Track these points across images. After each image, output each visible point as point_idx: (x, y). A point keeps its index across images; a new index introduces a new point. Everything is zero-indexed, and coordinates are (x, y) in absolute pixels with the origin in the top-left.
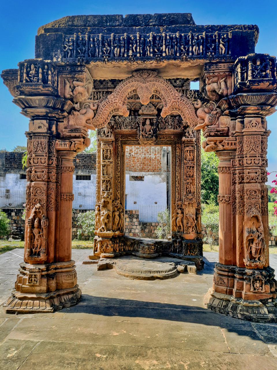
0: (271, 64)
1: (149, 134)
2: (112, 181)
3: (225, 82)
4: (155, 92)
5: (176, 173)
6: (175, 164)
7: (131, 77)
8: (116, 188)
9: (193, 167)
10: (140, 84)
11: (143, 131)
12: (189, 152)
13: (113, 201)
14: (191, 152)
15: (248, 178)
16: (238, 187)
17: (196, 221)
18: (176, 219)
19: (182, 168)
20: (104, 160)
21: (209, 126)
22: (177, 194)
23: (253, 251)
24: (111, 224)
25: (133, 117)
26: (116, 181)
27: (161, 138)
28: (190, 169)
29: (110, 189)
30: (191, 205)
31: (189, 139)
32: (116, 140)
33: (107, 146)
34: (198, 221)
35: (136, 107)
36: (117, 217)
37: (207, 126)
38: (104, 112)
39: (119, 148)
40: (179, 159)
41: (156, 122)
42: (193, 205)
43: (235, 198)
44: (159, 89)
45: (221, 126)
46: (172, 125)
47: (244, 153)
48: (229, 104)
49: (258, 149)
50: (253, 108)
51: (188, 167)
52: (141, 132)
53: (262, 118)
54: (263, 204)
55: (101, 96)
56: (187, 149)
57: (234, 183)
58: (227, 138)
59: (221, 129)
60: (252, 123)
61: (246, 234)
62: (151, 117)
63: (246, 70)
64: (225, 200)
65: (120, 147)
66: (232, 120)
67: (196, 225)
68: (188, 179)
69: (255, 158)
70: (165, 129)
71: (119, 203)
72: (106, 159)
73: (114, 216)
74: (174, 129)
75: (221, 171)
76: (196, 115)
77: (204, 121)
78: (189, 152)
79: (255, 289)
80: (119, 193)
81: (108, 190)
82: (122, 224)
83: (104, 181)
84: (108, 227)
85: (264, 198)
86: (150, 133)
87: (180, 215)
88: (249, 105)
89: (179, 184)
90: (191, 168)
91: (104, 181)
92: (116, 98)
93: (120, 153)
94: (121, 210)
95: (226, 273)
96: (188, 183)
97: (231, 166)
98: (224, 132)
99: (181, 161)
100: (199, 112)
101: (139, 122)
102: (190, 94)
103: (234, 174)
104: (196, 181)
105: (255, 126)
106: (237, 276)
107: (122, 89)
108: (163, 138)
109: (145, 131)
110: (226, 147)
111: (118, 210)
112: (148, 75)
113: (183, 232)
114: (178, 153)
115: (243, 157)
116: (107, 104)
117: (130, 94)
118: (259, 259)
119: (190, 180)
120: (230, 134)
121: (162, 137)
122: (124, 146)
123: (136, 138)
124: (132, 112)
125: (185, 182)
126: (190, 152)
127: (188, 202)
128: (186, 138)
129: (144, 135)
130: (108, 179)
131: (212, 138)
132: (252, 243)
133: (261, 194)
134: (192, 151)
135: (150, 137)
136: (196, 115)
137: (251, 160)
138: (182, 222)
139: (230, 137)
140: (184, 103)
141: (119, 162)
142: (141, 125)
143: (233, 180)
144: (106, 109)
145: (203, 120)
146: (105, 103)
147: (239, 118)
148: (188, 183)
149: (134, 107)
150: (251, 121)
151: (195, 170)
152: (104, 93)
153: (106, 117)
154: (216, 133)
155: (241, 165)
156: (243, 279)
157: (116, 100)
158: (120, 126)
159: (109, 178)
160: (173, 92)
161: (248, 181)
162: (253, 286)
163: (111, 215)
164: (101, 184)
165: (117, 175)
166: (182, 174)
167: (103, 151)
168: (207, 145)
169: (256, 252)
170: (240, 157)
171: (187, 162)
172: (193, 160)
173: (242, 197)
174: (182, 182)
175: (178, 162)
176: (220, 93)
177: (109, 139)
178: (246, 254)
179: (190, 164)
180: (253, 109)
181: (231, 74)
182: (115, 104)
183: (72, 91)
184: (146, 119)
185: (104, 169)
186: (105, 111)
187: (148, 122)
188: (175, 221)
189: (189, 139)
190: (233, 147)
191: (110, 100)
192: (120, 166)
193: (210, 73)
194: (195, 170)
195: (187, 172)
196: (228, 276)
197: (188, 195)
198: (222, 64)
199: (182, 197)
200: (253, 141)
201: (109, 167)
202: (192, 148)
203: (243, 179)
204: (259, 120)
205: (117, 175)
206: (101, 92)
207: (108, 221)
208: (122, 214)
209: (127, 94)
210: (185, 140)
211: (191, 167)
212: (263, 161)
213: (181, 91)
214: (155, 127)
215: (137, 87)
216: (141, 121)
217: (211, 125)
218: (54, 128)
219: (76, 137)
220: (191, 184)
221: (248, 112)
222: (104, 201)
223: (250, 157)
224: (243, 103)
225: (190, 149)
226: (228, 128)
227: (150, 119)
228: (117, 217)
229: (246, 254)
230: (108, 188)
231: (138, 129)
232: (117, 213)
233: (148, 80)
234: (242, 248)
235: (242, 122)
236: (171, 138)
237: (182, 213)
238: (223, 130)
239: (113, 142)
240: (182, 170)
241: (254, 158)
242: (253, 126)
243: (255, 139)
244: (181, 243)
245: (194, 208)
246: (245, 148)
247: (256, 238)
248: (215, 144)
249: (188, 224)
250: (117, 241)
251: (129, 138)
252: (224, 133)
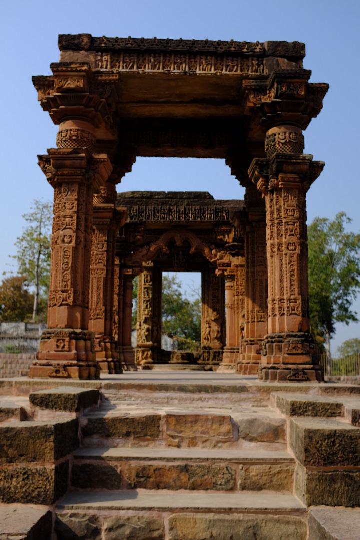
36: (155, 331)
91: (144, 301)
95: (229, 350)
183: (134, 239)
187: (181, 253)
196: (231, 352)
218: (122, 262)
219: (136, 267)
228: (155, 331)
244: (209, 352)
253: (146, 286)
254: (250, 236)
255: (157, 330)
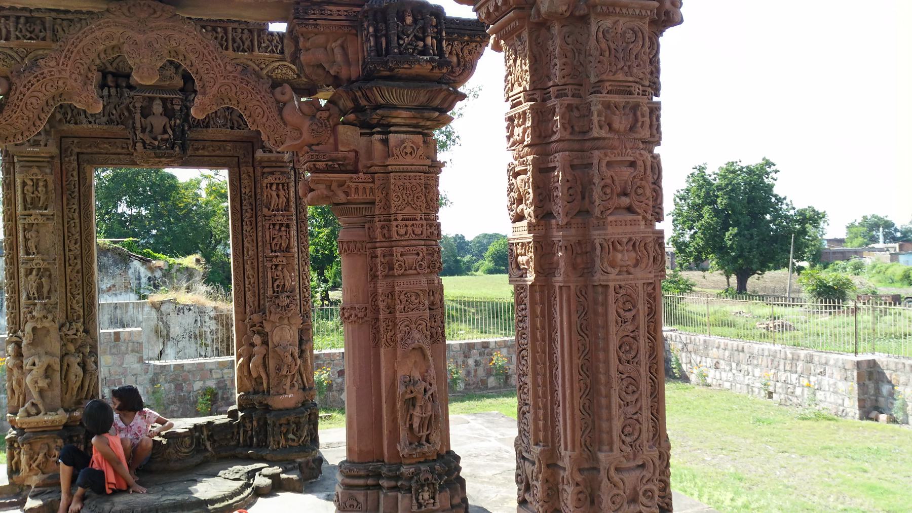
0: (434, 24)
1: (167, 140)
2: (56, 270)
3: (343, 47)
4: (173, 54)
5: (245, 241)
6: (239, 216)
7: (102, 13)
8: (69, 288)
9: (288, 226)
10: (130, 33)
11: (143, 130)
12: (274, 187)
13: (62, 326)
14: (281, 186)
15: (400, 266)
16: (382, 286)
17: (299, 361)
18: (250, 359)
19: (260, 229)
20: (27, 212)
21: (314, 148)
22: (248, 294)
23: (416, 425)
24: (57, 391)
25: (113, 91)
26: (69, 270)
27: (197, 149)
28: (280, 230)
29: (49, 292)
30: (286, 321)
31: (274, 155)
32: (63, 151)
33: (35, 170)
34: (305, 361)
35: (120, 64)
37: (310, 146)
38: (29, 103)
39: (72, 175)
40: (251, 204)
41: (181, 110)
42: (293, 321)
43: (376, 310)
44: (182, 47)
45: (341, 148)
46: (225, 117)
47: (393, 211)
48: (355, 100)
49: (418, 204)
50: (405, 114)
51: (274, 225)
52: (139, 135)
53: (425, 135)
54: (433, 320)
55: (12, 29)
56: (271, 179)
57: (374, 277)
58: (355, 176)
59: (340, 155)
60: (405, 147)
61: (400, 389)
62: (165, 96)
63: (384, 32)
64: (356, 316)
65: (75, 173)
66: (362, 134)
67: (299, 370)
68: (277, 257)
69: (414, 222)
70: (207, 126)
71: (81, 330)
72: (35, 208)
73: (65, 367)
74: (232, 128)
75: (345, 251)
76: (282, 118)
77: (301, 134)
78: (274, 187)
79: (420, 506)
80: (78, 303)
81: (45, 295)
82: (92, 388)
83: (32, 270)
84: (48, 401)
85: (435, 307)
86: (166, 136)
87: (259, 350)
88: (395, 107)
89: (253, 268)
90: (283, 229)
91: (29, 272)
92: (64, 67)
93: (77, 190)
94: (88, 350)
95: (361, 482)
96: (277, 266)
97: (367, 239)
98: (347, 162)
99: (255, 209)
100: (286, 112)
101: (131, 106)
102: (271, 41)
103: (372, 257)
104: (296, 260)
105: (411, 153)
106: (384, 483)
107: (81, 45)
108: (203, 149)
109: (151, 131)
110: (353, 197)
111: (78, 350)
112: (151, 11)
113: (269, 392)
114: (248, 190)
115: (390, 221)
116: (38, 81)
117: (103, 56)
118: (428, 441)
119: (281, 259)
120: (360, 167)
121: (201, 146)
122: (88, 167)
123: (123, 148)
124: (110, 79)
125: (269, 264)
126: (277, 189)
127: (278, 316)
128: (264, 152)
129: (148, 142)
130: (43, 265)
131: (321, 175)
132: (414, 406)
133: (429, 300)
134: (283, 184)
135: (167, 148)
136: (282, 118)
137: (406, 226)
138: (265, 366)
139: (361, 175)
140: (249, 88)
141: (76, 215)
142: (138, 116)
143: (371, 270)
144: (35, 93)
145: (298, 129)
146: (31, 78)
147: (378, 133)
148: (277, 266)
149: (114, 65)
150: (403, 142)
151: (293, 232)
152: (22, 20)
153: (36, 114)
154: (330, 163)
155: (389, 239)
156: (395, 488)
157: (63, 73)
158: (72, 116)
159: (46, 263)
160: (219, 61)
161: (401, 272)
162: (417, 499)
163: (57, 367)
164: (22, 280)
165: (70, 250)
166: (260, 244)
167: (24, 184)
168: (312, 190)
169: (421, 426)
170: (385, 221)
171: (270, 213)
172: (287, 208)
173: (391, 310)
174: (260, 265)
175: (247, 211)
176: (332, 72)
177: (38, 152)
178: (403, 434)
179: (280, 217)
180: (404, 116)
181: (354, 32)
182: (61, 82)
184: (152, 99)
185: (28, 235)
186: (34, 101)
187: (157, 108)
188: (246, 367)
189: (274, 155)
190: (369, 197)
191: (46, 71)
192: (78, 225)
193: (307, 25)
194: (293, 232)
195: (274, 239)
196: (367, 487)
197: (277, 297)
198: (334, 8)
199: (262, 302)
200: (409, 186)
201: (43, 230)
202: (284, 179)
203: (391, 268)
204: (419, 139)
205: (70, 250)
206: (12, 19)
207: (49, 385)
208: (93, 359)
209: (93, 56)
210: (262, 158)
211: (281, 225)
212: (431, 226)
213: (246, 31)
214: (178, 121)
215: (122, 41)
216: (138, 105)
217: (318, 144)
220: (285, 270)
221: (394, 121)
222: (34, 329)
223: (402, 220)
224: (382, 102)
225: (278, 181)
226: (356, 152)
227: (164, 101)
228: (76, 370)
229: (403, 434)
230: (45, 290)
231: (131, 126)
232: (74, 360)
233: (153, 25)
234: (394, 421)
235: (385, 142)
236: (225, 149)
237: (265, 343)
238: (345, 158)
239: (52, 157)
240: (260, 234)
241: (411, 222)
242: (406, 153)
243: (413, 180)
245: (295, 328)
246: (395, 202)
247: (420, 396)
248: (329, 187)
249: (279, 369)
250: (78, 436)
251: (102, 146)
252: (348, 164)
253: (31, 220)
254: (556, 45)
255: (83, 365)
